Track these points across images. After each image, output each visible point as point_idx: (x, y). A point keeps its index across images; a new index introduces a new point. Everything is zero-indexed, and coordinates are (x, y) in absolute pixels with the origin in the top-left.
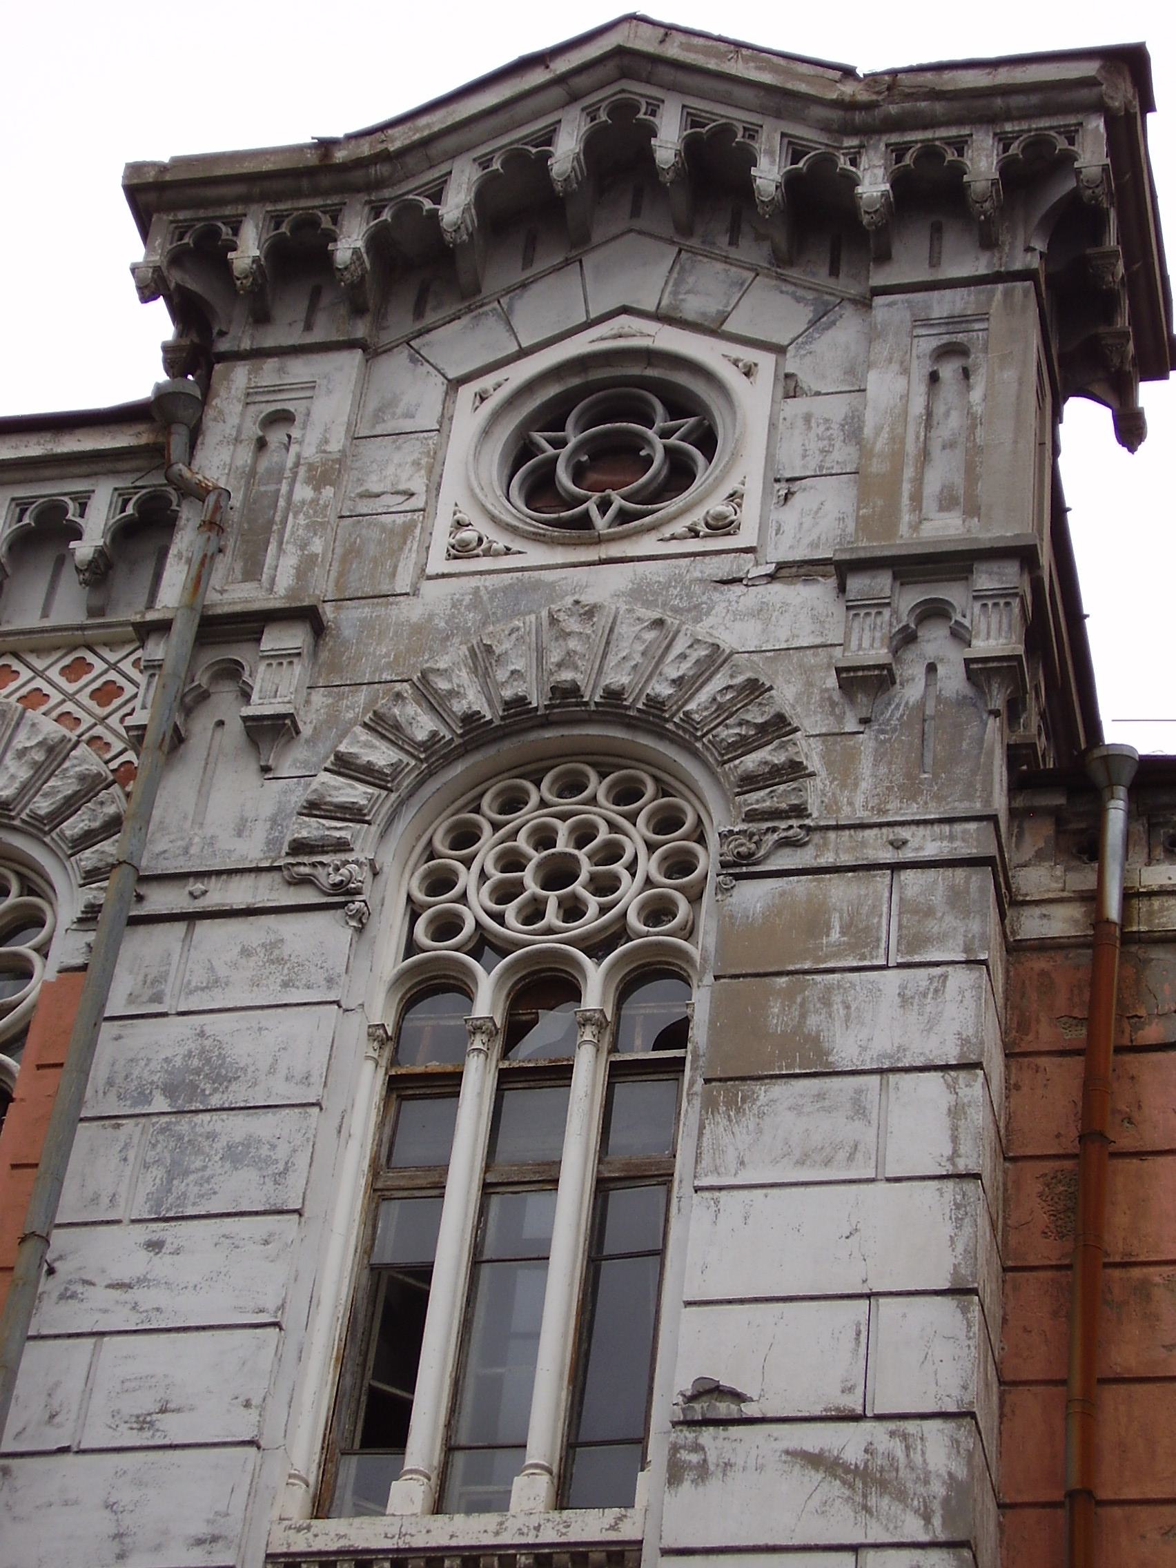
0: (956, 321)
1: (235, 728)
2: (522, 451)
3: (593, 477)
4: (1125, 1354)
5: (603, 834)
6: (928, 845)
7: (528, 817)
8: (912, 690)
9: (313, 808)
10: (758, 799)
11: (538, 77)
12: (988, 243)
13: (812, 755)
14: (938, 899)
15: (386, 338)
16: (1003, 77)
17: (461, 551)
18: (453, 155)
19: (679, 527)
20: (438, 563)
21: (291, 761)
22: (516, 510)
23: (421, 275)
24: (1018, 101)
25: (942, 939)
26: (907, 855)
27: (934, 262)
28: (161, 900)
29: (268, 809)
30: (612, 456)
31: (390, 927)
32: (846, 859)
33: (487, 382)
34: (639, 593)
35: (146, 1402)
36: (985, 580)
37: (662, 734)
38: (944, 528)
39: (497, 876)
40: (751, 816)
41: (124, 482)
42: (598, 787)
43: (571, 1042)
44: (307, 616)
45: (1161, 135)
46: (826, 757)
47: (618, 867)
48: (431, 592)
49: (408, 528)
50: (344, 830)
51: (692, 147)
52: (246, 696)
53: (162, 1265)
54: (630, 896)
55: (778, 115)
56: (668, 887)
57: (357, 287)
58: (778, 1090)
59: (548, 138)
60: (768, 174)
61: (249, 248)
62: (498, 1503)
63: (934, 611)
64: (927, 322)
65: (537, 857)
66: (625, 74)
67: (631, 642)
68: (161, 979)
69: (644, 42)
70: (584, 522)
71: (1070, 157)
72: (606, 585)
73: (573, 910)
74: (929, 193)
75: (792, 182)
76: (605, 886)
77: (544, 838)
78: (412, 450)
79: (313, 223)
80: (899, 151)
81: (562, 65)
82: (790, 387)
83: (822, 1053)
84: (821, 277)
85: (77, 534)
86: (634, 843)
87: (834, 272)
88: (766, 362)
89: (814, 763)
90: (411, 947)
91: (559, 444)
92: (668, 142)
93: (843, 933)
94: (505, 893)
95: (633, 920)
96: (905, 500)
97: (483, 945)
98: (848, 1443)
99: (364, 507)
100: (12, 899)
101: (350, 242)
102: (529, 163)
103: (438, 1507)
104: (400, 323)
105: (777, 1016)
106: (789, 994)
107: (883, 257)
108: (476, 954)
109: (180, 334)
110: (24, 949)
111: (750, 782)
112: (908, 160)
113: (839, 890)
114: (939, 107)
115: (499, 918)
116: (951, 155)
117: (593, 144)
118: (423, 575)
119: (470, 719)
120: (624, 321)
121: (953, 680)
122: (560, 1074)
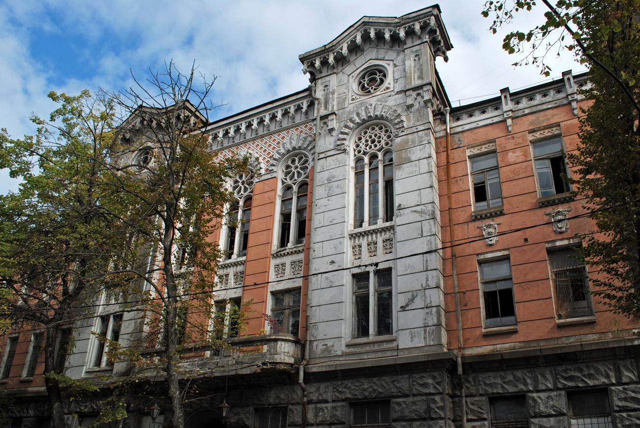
0: (417, 51)
1: (327, 131)
2: (360, 83)
3: (370, 84)
4: (455, 189)
5: (378, 135)
6: (422, 128)
7: (368, 134)
8: (417, 106)
9: (339, 140)
10: (397, 126)
11: (352, 29)
12: (420, 38)
13: (403, 118)
14: (423, 135)
15: (339, 71)
16: (418, 13)
17: (353, 99)
18: (343, 43)
19: (382, 89)
21: (334, 133)
22: (360, 92)
23: (341, 60)
24: (421, 17)
25: (424, 140)
26: (419, 130)
27: (413, 43)
28: (322, 156)
29: (333, 141)
30: (373, 80)
31: (352, 153)
32: (411, 132)
33: (353, 74)
34: (378, 101)
35: (331, 219)
36: (425, 88)
37: (384, 120)
38: (418, 82)
39: (365, 143)
40: (397, 129)
41: (307, 100)
42: (377, 128)
43: (378, 163)
45: (444, 17)
46: (407, 119)
47: (381, 139)
48: (350, 107)
49: (346, 98)
50: (344, 142)
51: (376, 34)
52: (328, 126)
53: (330, 202)
54: (383, 143)
55: (387, 26)
56: (388, 140)
57: (333, 65)
58: (405, 165)
59: (355, 37)
60: (387, 36)
61: (318, 64)
62: (376, 223)
63: (419, 94)
64: (413, 52)
65: (370, 140)
66: (365, 25)
67: (379, 108)
68: (324, 166)
69: (366, 20)
70: (370, 91)
71: (429, 23)
72: (373, 101)
73: (376, 146)
74: (410, 33)
75: (391, 36)
76: (379, 142)
77: (370, 137)
78: (344, 86)
79: (325, 57)
80: (405, 28)
81: (355, 26)
82: (395, 66)
83: (410, 159)
84: (398, 48)
85: (302, 108)
86: (382, 136)
87: (399, 47)
88: (391, 63)
89: (405, 120)
90: (355, 155)
91: (364, 81)
92: (372, 35)
93: (412, 142)
94: (366, 146)
95: (384, 146)
96: (413, 79)
97: (365, 153)
99: (339, 96)
100: (304, 158)
101: (331, 60)
102: (353, 42)
103: (369, 225)
104: (340, 68)
105: (404, 155)
106: (405, 152)
107: (405, 44)
108: (364, 154)
109: (311, 76)
110: (307, 165)
111: (396, 124)
112: (407, 29)
113: (410, 137)
114: (410, 20)
115: (366, 149)
116: (413, 27)
117: (362, 37)
118: (349, 104)
119: (358, 123)
120: (371, 61)
121: (422, 103)
122: (377, 168)
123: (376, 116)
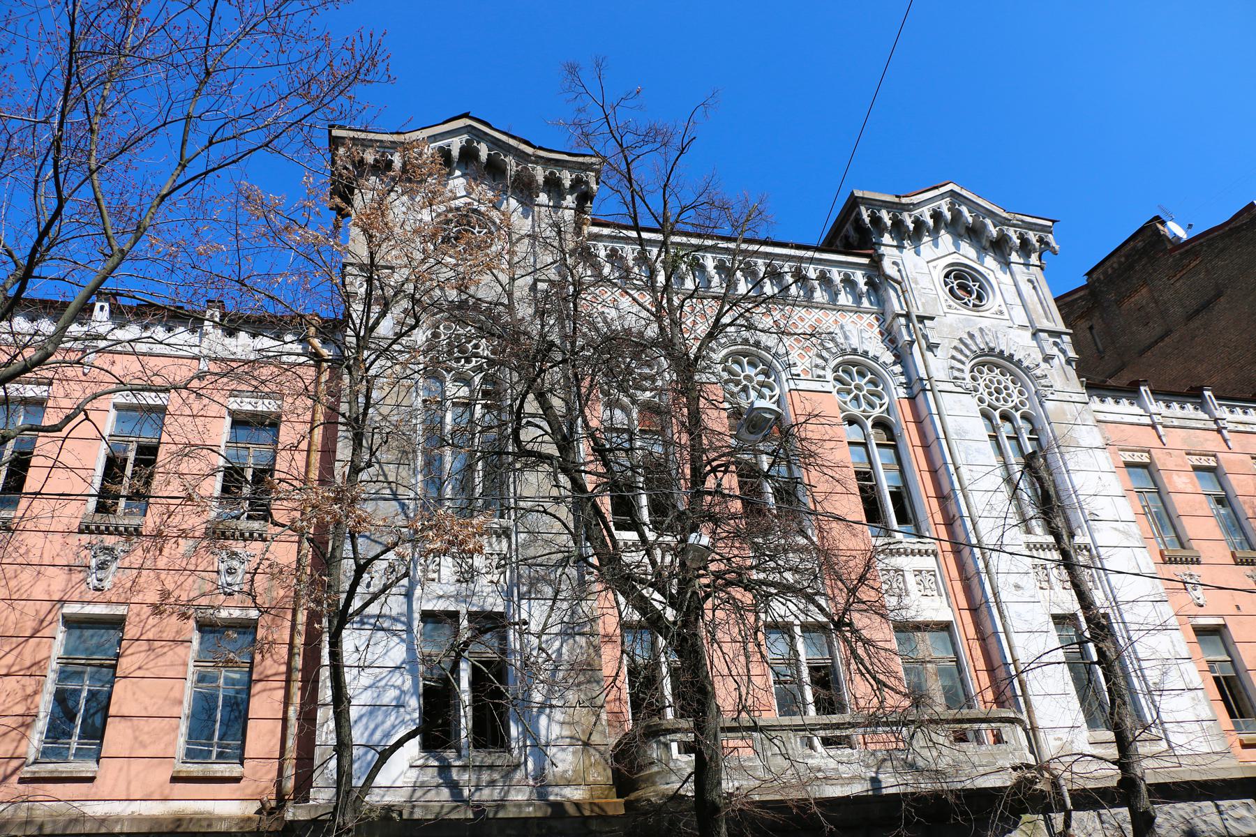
2: (946, 284)
20: (946, 310)
21: (939, 352)
44: (932, 319)
94: (990, 394)
98: (1119, 525)
123: (1002, 352)
